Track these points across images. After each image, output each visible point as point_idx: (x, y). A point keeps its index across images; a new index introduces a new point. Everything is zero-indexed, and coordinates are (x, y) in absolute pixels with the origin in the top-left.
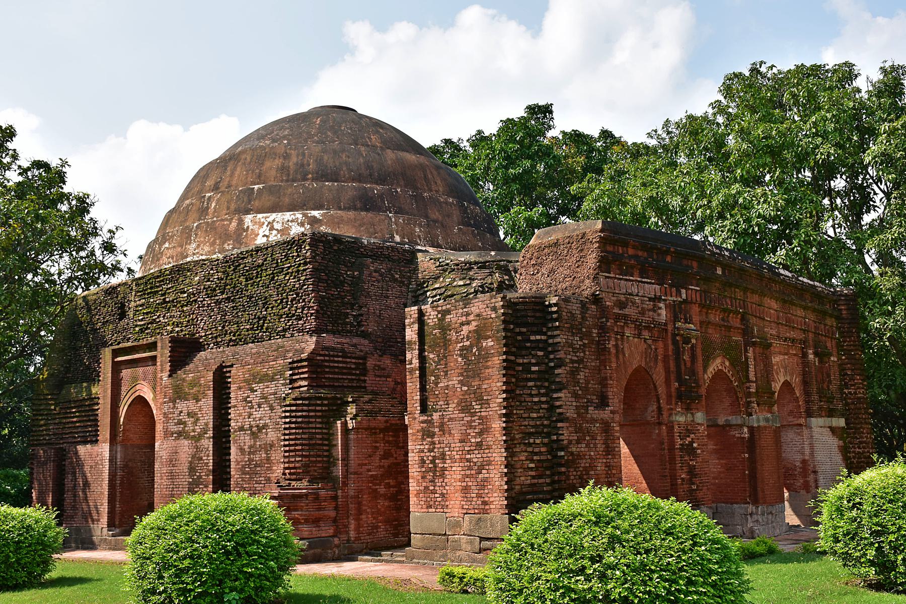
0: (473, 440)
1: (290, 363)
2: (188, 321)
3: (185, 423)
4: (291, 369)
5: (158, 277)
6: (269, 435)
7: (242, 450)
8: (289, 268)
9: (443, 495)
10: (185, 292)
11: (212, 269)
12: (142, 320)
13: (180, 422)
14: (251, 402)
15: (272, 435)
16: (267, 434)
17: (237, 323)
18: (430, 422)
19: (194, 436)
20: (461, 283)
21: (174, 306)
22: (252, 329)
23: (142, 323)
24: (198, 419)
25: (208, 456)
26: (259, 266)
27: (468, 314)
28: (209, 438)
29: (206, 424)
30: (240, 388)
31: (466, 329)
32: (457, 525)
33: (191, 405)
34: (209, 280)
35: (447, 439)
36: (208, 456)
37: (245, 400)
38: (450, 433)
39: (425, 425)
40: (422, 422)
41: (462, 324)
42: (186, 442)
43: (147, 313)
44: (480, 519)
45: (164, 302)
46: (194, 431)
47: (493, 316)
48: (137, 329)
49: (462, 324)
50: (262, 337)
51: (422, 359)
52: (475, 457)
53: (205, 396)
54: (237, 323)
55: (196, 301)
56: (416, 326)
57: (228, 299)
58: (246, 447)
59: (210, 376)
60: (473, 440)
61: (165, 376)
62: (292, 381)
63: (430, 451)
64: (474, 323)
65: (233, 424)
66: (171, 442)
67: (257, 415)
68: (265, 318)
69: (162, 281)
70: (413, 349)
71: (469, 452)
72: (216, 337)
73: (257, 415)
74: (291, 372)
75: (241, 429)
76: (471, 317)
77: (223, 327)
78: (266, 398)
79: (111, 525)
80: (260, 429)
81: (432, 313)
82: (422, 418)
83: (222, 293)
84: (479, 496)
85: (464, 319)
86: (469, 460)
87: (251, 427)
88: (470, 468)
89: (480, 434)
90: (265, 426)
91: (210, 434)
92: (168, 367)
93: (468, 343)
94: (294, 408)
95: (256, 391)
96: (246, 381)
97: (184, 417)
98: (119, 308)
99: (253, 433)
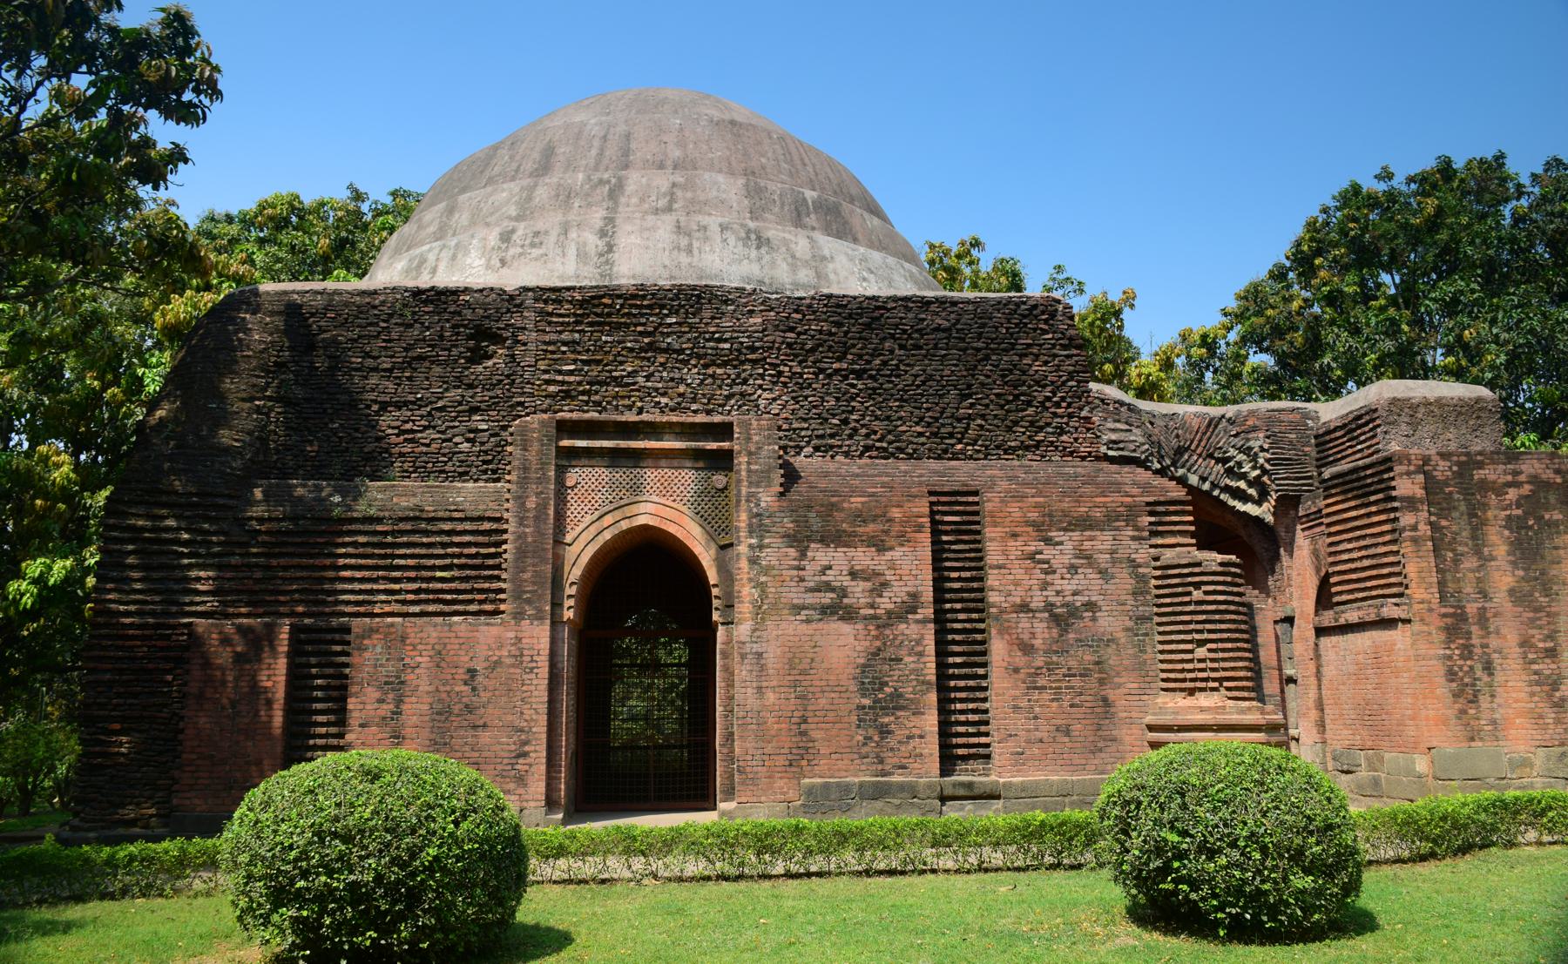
0: (1541, 645)
1: (1148, 504)
2: (729, 397)
3: (843, 593)
4: (1151, 514)
5: (634, 297)
6: (1101, 622)
7: (1027, 649)
8: (1029, 345)
9: (1494, 722)
10: (726, 341)
11: (796, 311)
12: (571, 373)
13: (828, 587)
14: (1047, 562)
15: (1110, 622)
16: (1094, 619)
17: (888, 418)
18: (1461, 617)
19: (875, 617)
20: (1118, 426)
21: (685, 362)
22: (935, 435)
23: (572, 379)
24: (885, 585)
25: (921, 654)
26: (938, 329)
27: (1516, 473)
28: (924, 621)
29: (914, 596)
30: (1015, 535)
31: (1512, 494)
32: (1526, 763)
33: (863, 557)
34: (792, 330)
35: (1494, 642)
36: (921, 654)
37: (1031, 557)
38: (1497, 632)
39: (1449, 620)
40: (1445, 615)
41: (1510, 485)
42: (846, 628)
43: (585, 362)
44: (1563, 754)
45: (651, 347)
46: (872, 606)
47: (1559, 480)
48: (552, 388)
49: (1510, 485)
50: (963, 452)
51: (1431, 523)
52: (1546, 667)
53: (903, 539)
54: (888, 418)
55: (754, 362)
56: (1421, 478)
57: (859, 375)
58: (1038, 643)
59: (922, 507)
60: (1541, 645)
61: (767, 498)
62: (1154, 534)
63: (1462, 657)
64: (1527, 487)
65: (993, 597)
66: (793, 627)
67: (1068, 586)
68: (969, 417)
69: (650, 307)
70: (1417, 510)
71: (1533, 662)
72: (822, 437)
73: (1068, 586)
74: (1153, 519)
75: (1024, 607)
76: (1522, 478)
77: (845, 422)
78: (1088, 557)
79: (551, 803)
80: (1073, 612)
81: (1441, 463)
82: (1444, 610)
83: (839, 360)
84: (1558, 721)
85: (1509, 478)
86: (1536, 673)
87: (1049, 607)
88: (1538, 683)
89: (1550, 637)
90: (1091, 606)
91: (929, 612)
92: (777, 477)
93: (1519, 512)
94: (1229, 579)
95: (1061, 543)
96: (1035, 525)
97: (838, 577)
98: (470, 337)
99: (1056, 619)
